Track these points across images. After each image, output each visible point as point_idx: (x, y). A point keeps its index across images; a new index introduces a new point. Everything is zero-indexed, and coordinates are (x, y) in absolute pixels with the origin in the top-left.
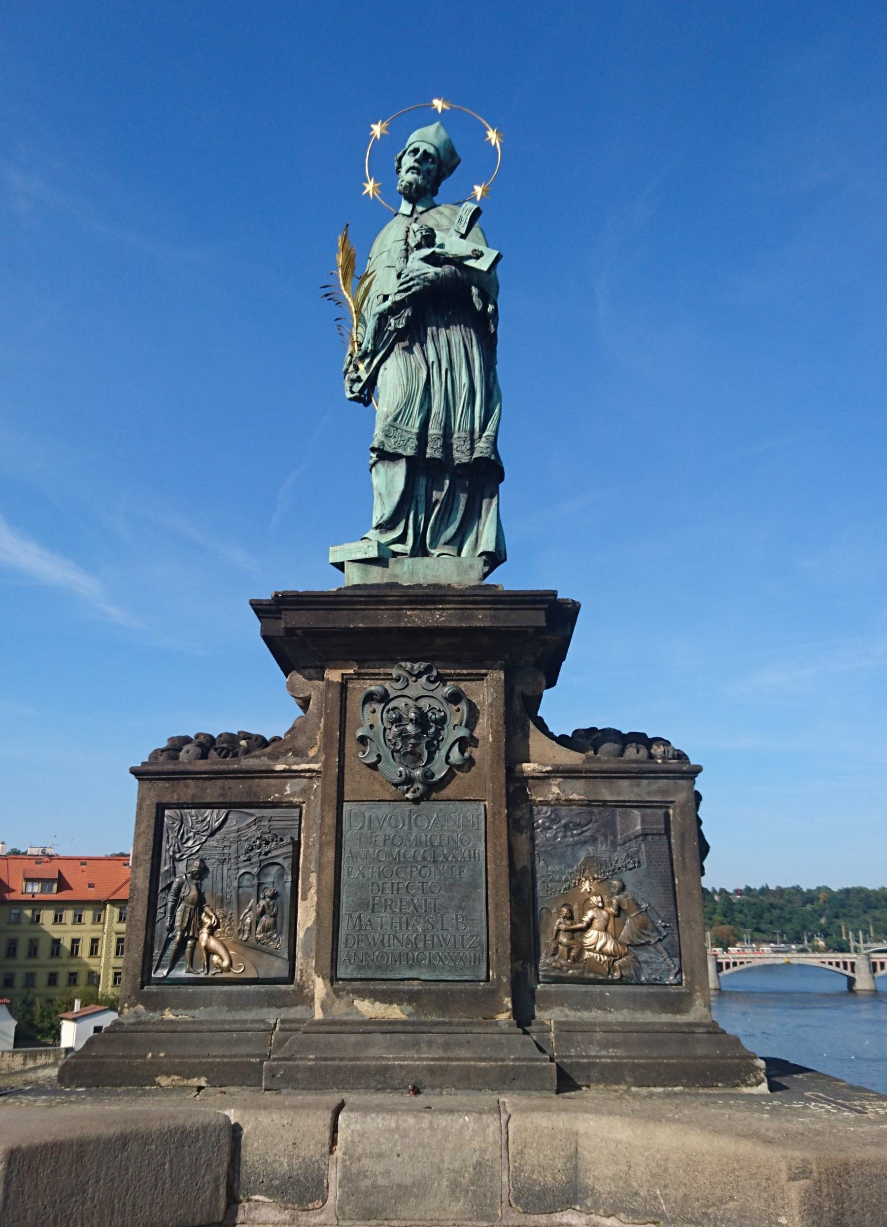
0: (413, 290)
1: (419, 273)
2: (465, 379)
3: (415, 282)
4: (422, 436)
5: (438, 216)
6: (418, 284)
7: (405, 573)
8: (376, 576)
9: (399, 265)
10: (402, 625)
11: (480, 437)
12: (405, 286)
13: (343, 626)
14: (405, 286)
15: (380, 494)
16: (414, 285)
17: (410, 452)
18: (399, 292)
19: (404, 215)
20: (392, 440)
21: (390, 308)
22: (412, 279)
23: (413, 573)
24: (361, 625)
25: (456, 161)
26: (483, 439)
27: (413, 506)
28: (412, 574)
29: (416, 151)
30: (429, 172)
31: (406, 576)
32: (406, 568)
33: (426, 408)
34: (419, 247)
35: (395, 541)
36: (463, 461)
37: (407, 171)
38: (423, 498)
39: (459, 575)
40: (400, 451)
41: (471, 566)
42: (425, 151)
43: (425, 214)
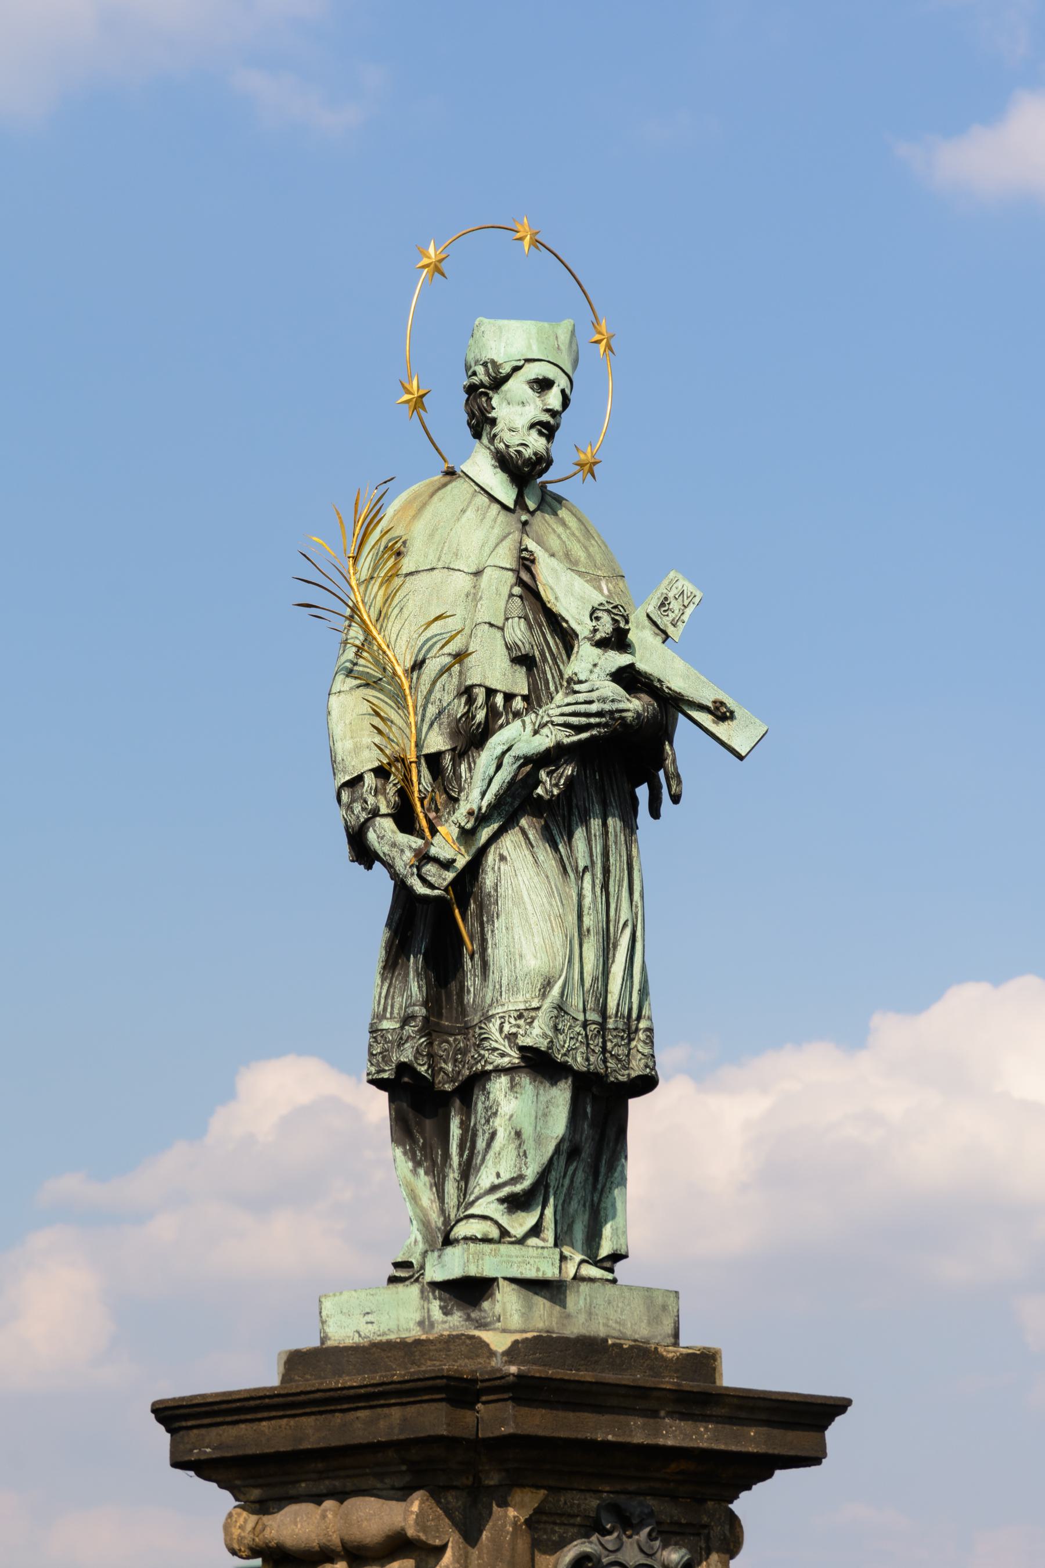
0: (594, 732)
1: (615, 706)
3: (603, 720)
5: (560, 530)
6: (605, 725)
7: (579, 1311)
8: (543, 1316)
9: (518, 632)
10: (661, 1441)
11: (637, 1030)
12: (583, 720)
13: (589, 1436)
14: (583, 720)
15: (518, 1134)
16: (598, 725)
17: (578, 1062)
18: (566, 725)
19: (493, 499)
20: (561, 1037)
22: (599, 714)
23: (590, 1314)
24: (610, 1437)
26: (641, 1035)
28: (590, 1314)
29: (543, 385)
31: (582, 1318)
32: (582, 1303)
36: (620, 1077)
37: (532, 426)
39: (649, 1323)
40: (570, 1060)
43: (538, 512)
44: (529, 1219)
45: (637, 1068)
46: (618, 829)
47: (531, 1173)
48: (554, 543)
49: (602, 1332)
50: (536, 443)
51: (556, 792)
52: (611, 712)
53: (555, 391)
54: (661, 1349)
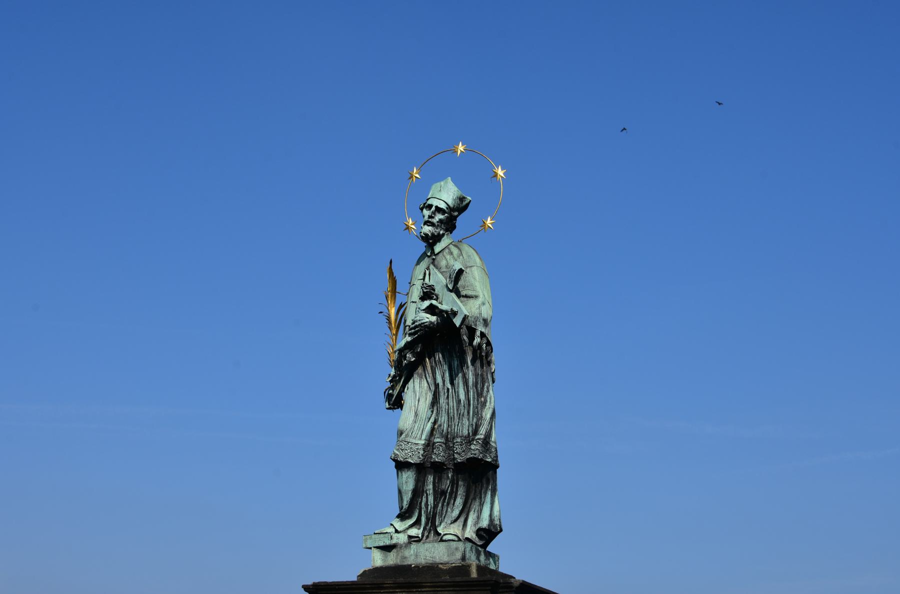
2: (462, 397)
4: (429, 445)
5: (448, 257)
8: (392, 559)
11: (473, 440)
21: (405, 345)
25: (464, 203)
27: (424, 499)
30: (441, 221)
31: (413, 558)
32: (412, 552)
33: (432, 420)
34: (423, 299)
35: (411, 526)
38: (431, 491)
40: (410, 460)
41: (457, 549)
42: (437, 207)
44: (411, 522)
45: (469, 455)
46: (456, 363)
47: (405, 504)
48: (443, 263)
49: (423, 562)
50: (427, 229)
51: (413, 360)
52: (420, 325)
53: (433, 208)
54: (440, 566)
